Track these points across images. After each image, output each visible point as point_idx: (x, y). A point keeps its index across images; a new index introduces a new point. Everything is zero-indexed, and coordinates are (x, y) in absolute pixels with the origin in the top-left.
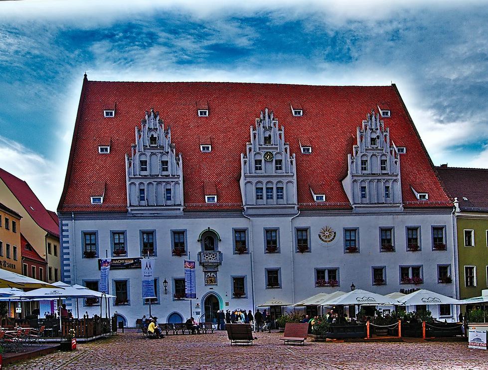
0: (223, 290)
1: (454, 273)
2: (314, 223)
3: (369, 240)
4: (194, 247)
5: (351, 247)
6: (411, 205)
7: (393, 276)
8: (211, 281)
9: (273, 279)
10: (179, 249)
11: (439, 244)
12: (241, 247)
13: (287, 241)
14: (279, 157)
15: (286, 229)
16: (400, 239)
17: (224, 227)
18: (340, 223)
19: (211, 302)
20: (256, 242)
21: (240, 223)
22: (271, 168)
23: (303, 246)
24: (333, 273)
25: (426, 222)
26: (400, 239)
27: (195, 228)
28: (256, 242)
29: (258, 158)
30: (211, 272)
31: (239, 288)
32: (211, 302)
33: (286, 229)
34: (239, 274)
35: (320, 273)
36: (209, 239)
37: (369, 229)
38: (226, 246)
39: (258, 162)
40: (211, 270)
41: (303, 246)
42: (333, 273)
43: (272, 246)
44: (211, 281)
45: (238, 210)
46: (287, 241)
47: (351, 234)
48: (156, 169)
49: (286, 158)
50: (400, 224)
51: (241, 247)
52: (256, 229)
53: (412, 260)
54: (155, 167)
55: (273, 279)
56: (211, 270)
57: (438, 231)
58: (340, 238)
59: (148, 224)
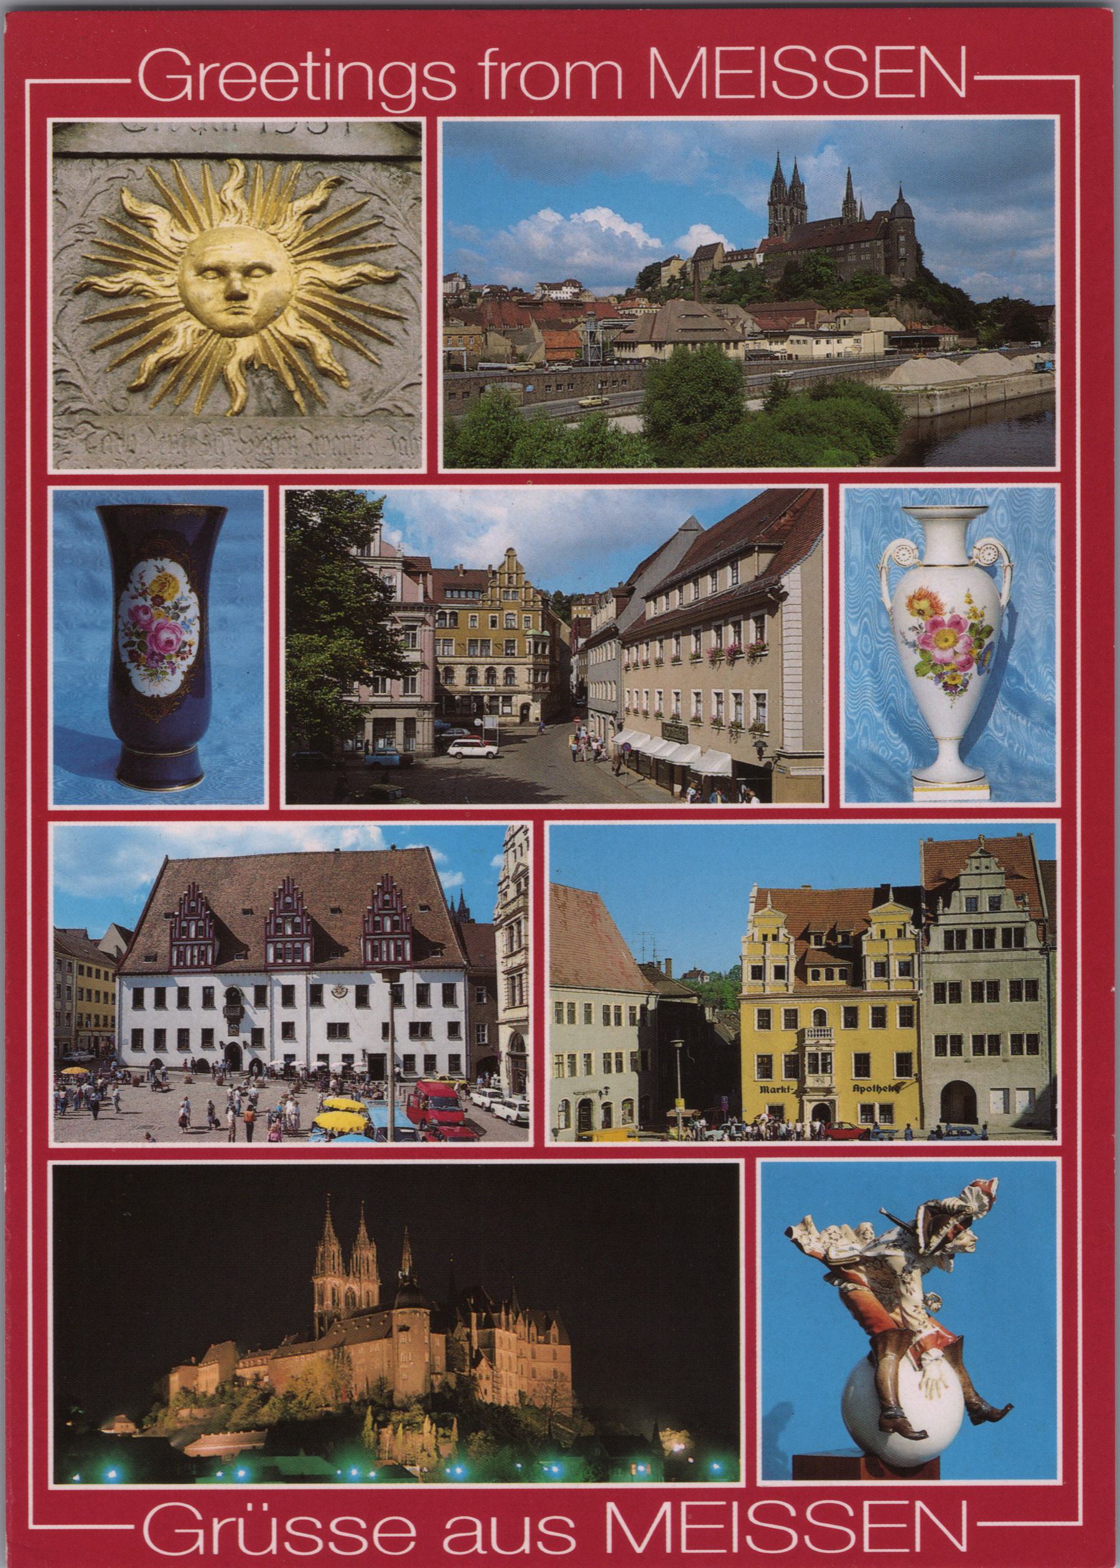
4: (220, 1001)
5: (362, 999)
7: (402, 1030)
10: (208, 1000)
11: (449, 998)
13: (301, 996)
21: (260, 979)
44: (234, 1032)
46: (301, 996)
53: (421, 1015)
55: (288, 1030)
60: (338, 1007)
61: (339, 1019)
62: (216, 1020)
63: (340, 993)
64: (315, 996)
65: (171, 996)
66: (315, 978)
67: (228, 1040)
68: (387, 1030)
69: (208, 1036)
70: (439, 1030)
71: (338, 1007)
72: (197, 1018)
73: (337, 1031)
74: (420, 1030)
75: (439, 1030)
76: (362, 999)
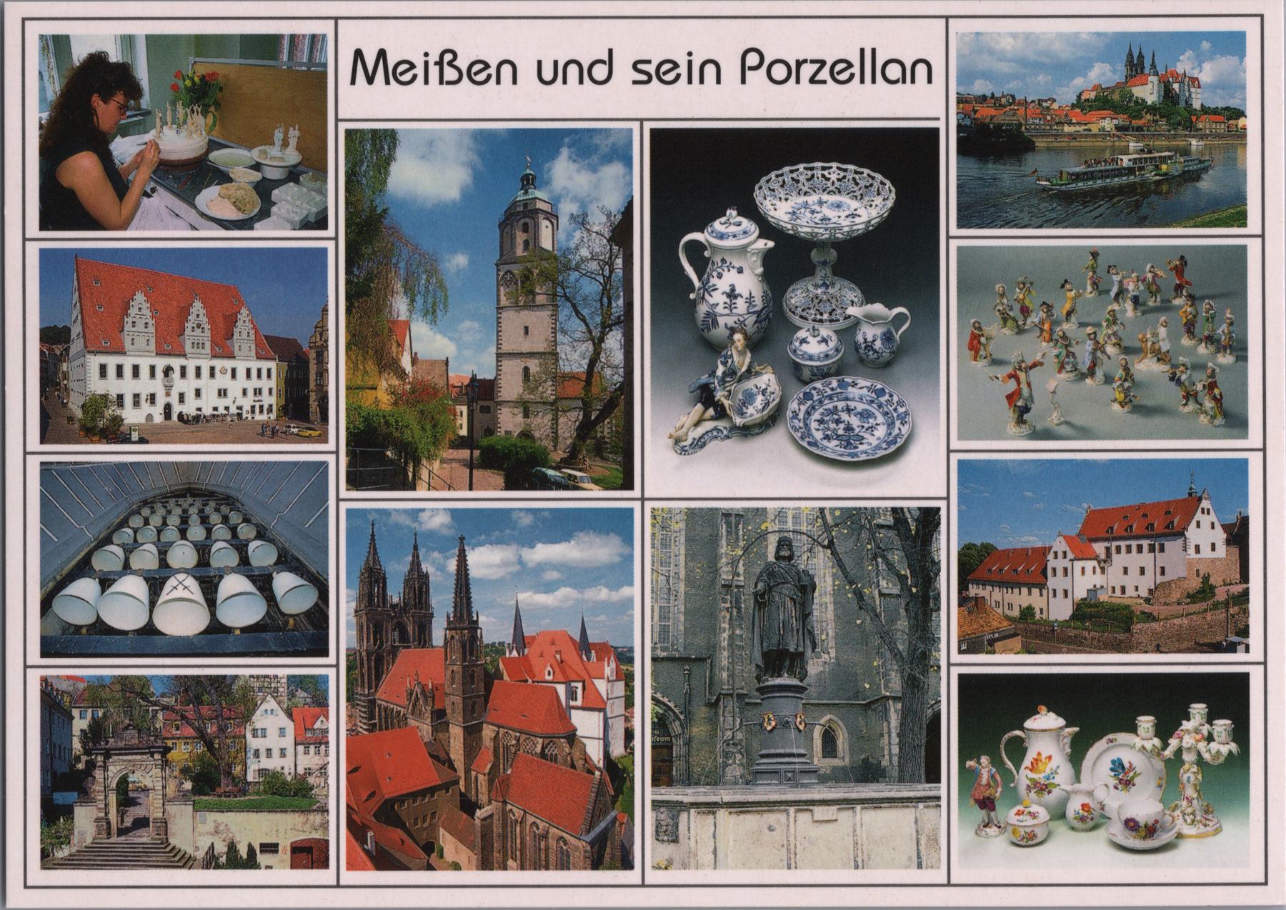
0: (174, 400)
1: (274, 391)
3: (241, 373)
5: (234, 376)
6: (259, 358)
9: (198, 393)
11: (269, 376)
13: (205, 372)
15: (205, 365)
16: (254, 373)
18: (228, 364)
19: (168, 408)
20: (191, 372)
21: (182, 361)
24: (225, 391)
25: (265, 365)
26: (254, 373)
27: (161, 363)
28: (191, 372)
31: (182, 398)
32: (168, 408)
33: (205, 365)
35: (220, 391)
37: (241, 367)
40: (168, 388)
41: (212, 375)
42: (225, 391)
44: (168, 394)
45: (183, 355)
46: (205, 372)
47: (234, 371)
49: (207, 327)
50: (254, 365)
52: (191, 365)
54: (140, 326)
55: (198, 393)
56: (168, 388)
57: (269, 371)
58: (229, 372)
59: (136, 361)
63: (224, 372)
64: (212, 375)
65: (128, 371)
68: (245, 392)
69: (152, 399)
70: (265, 392)
71: (223, 381)
72: (145, 385)
73: (222, 393)
74: (258, 392)
75: (265, 392)
76: (234, 376)
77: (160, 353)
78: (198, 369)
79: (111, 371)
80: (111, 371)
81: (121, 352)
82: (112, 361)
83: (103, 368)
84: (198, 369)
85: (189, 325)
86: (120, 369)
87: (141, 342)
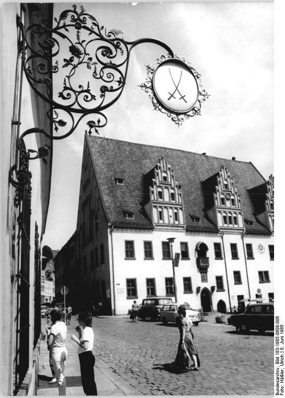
2: (255, 242)
8: (204, 279)
9: (237, 276)
12: (219, 255)
14: (232, 197)
17: (209, 241)
21: (218, 240)
22: (228, 204)
23: (250, 255)
24: (266, 273)
27: (193, 241)
29: (222, 196)
30: (204, 272)
34: (219, 274)
36: (202, 250)
38: (211, 253)
39: (223, 200)
42: (266, 273)
43: (235, 256)
44: (204, 279)
48: (167, 198)
51: (219, 255)
54: (167, 198)
55: (237, 276)
60: (261, 261)
61: (263, 269)
62: (188, 268)
66: (248, 240)
67: (203, 285)
77: (190, 230)
78: (234, 247)
79: (139, 250)
80: (139, 250)
81: (147, 225)
82: (139, 239)
83: (129, 245)
84: (234, 247)
85: (219, 196)
86: (148, 245)
87: (168, 214)
